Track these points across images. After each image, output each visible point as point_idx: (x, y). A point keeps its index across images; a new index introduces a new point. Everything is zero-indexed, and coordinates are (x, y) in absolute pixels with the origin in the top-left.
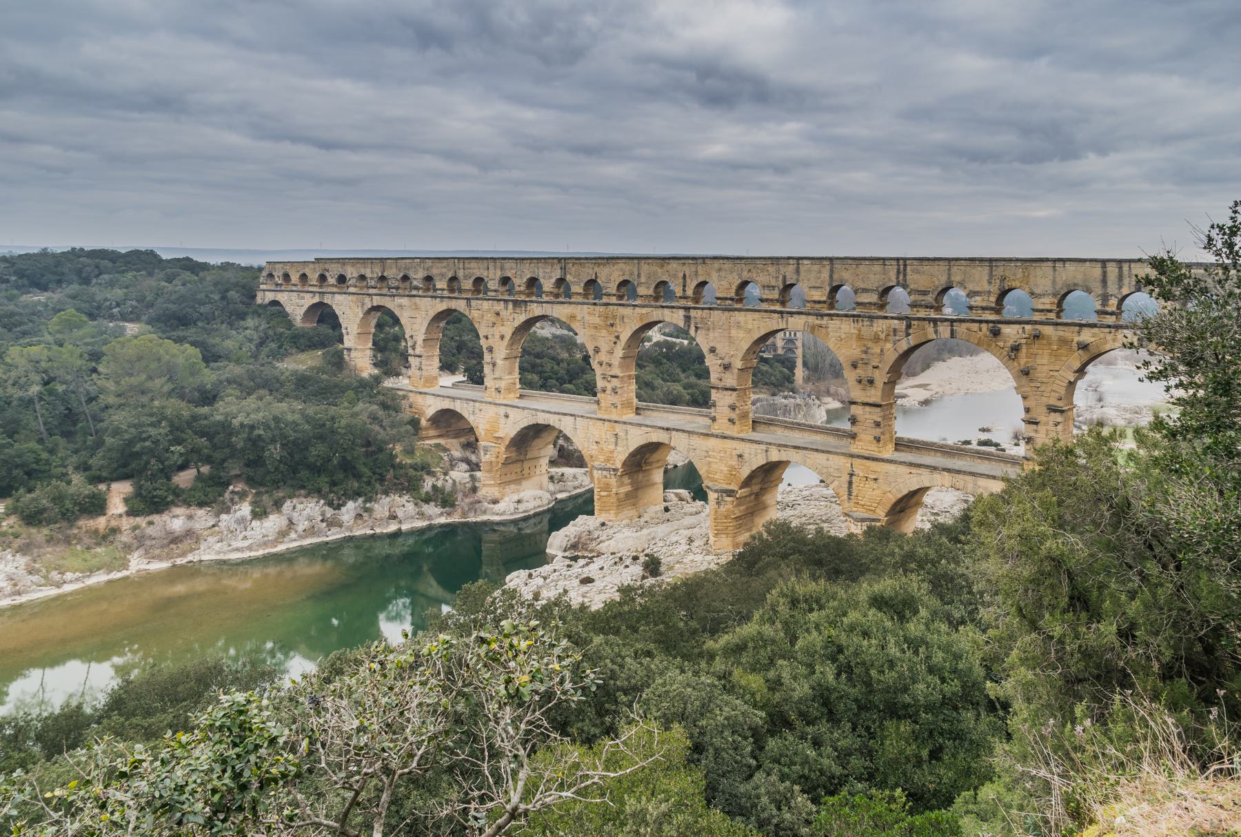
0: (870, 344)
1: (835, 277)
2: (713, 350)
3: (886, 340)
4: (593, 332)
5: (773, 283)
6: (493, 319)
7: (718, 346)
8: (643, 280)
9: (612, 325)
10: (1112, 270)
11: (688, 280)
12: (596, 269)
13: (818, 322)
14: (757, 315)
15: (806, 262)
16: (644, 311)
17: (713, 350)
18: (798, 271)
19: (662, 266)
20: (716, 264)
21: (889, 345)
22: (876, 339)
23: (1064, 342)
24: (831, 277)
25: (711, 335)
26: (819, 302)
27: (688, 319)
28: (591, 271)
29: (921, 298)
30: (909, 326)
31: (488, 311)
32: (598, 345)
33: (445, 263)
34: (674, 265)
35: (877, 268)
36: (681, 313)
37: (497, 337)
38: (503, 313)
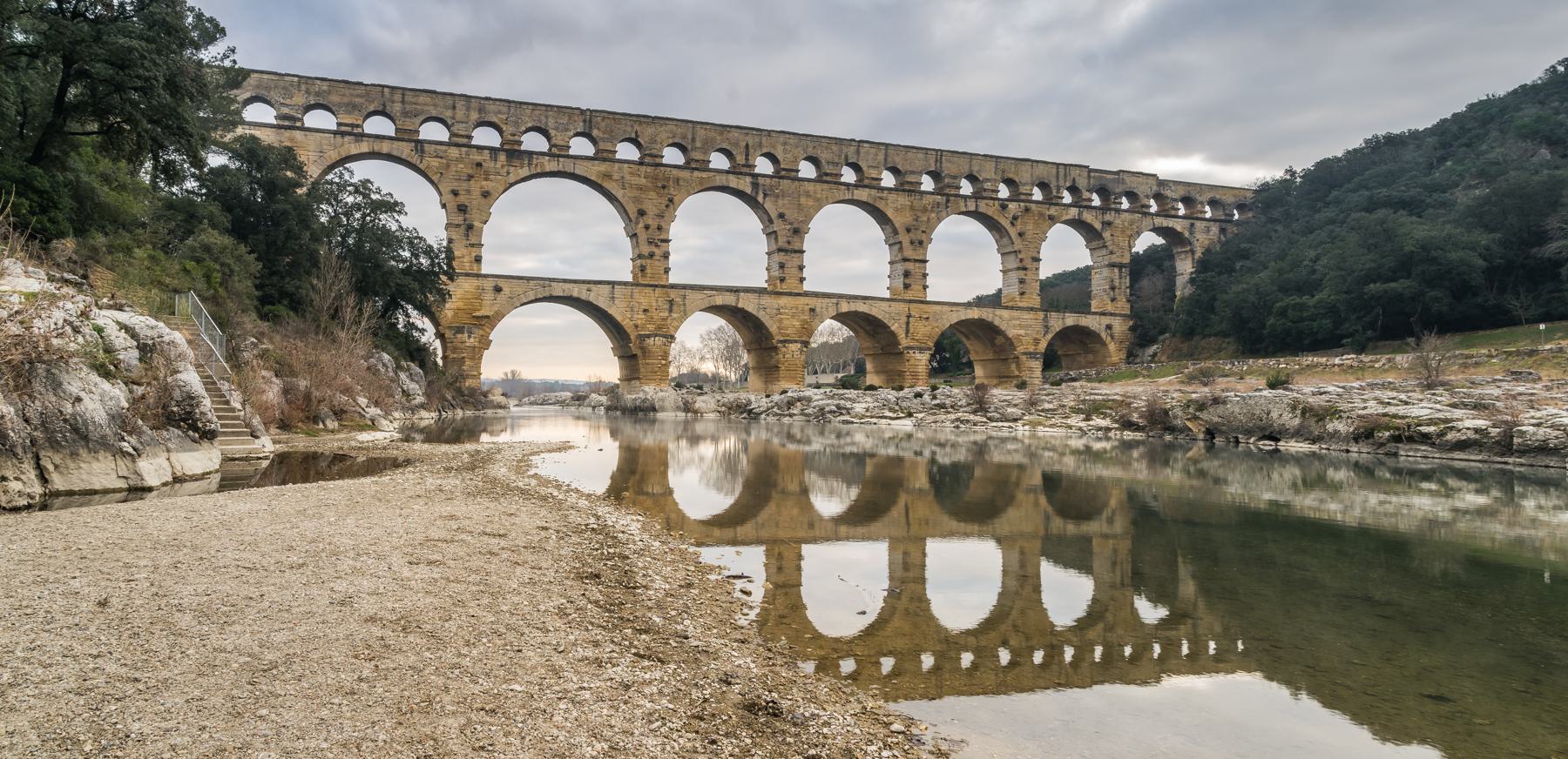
2: (781, 216)
4: (636, 193)
8: (698, 144)
10: (1061, 169)
12: (637, 127)
17: (781, 216)
18: (858, 152)
19: (721, 134)
20: (782, 138)
23: (1041, 215)
25: (780, 202)
27: (755, 185)
31: (459, 160)
32: (644, 207)
33: (361, 91)
34: (736, 134)
36: (748, 179)
37: (476, 193)
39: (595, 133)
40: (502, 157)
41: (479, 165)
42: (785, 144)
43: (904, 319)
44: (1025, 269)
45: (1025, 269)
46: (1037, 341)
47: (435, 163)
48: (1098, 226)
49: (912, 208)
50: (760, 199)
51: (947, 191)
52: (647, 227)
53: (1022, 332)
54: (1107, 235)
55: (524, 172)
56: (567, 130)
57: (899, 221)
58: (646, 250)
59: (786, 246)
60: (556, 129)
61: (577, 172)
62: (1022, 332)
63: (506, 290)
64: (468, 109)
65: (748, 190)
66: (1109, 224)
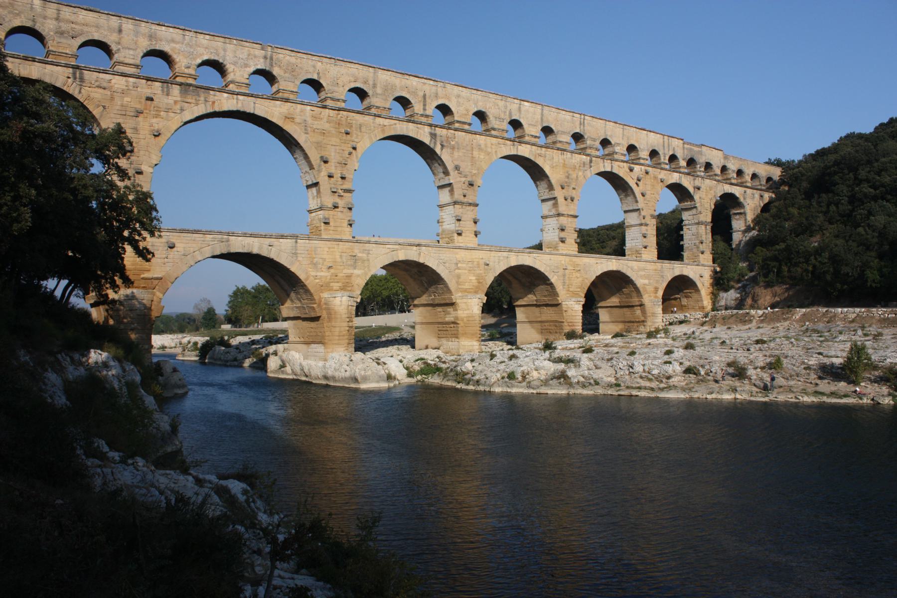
0: (571, 172)
1: (545, 119)
2: (457, 168)
3: (579, 170)
5: (502, 116)
6: (138, 106)
7: (463, 166)
8: (379, 90)
9: (347, 133)
11: (428, 100)
13: (539, 152)
14: (494, 140)
15: (526, 104)
16: (387, 122)
17: (457, 168)
20: (457, 90)
21: (580, 173)
22: (574, 168)
23: (655, 178)
24: (542, 119)
25: (456, 154)
26: (536, 137)
27: (433, 136)
28: (311, 70)
29: (593, 143)
30: (591, 161)
32: (325, 154)
34: (414, 81)
35: (567, 116)
36: (427, 129)
38: (162, 100)
39: (276, 71)
40: (176, 90)
41: (150, 99)
42: (458, 96)
43: (561, 272)
44: (646, 225)
45: (646, 225)
46: (656, 289)
47: (97, 94)
48: (691, 190)
49: (564, 165)
50: (438, 150)
51: (588, 151)
52: (330, 176)
53: (646, 281)
54: (696, 197)
55: (201, 110)
56: (246, 66)
57: (555, 176)
58: (329, 201)
59: (462, 199)
60: (235, 64)
61: (259, 113)
62: (646, 281)
63: (180, 246)
64: (137, 34)
65: (427, 140)
66: (699, 189)
